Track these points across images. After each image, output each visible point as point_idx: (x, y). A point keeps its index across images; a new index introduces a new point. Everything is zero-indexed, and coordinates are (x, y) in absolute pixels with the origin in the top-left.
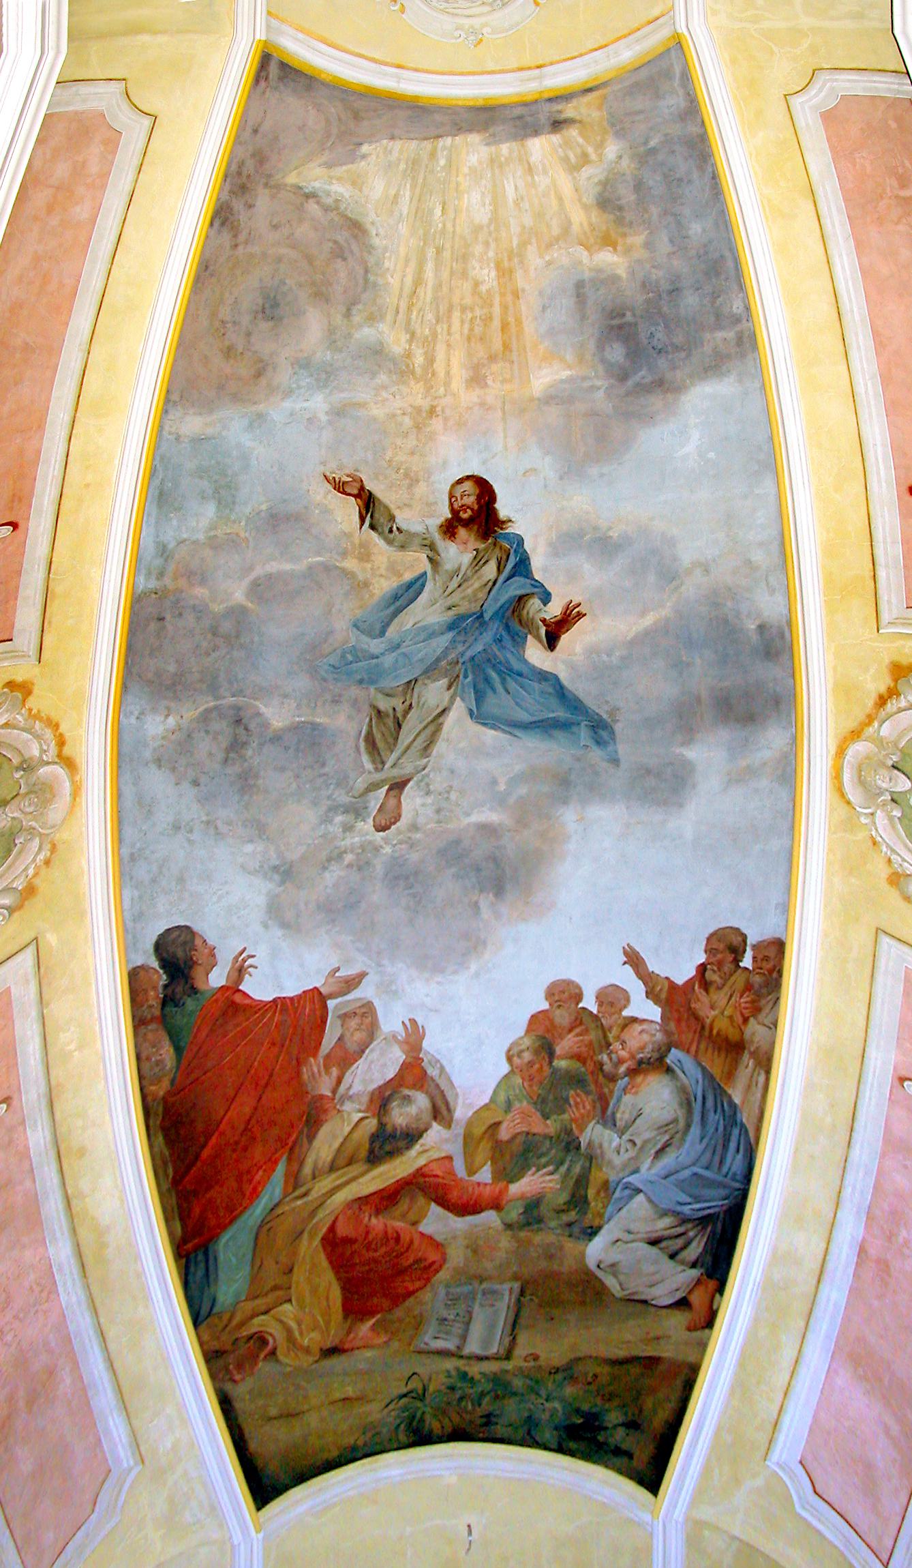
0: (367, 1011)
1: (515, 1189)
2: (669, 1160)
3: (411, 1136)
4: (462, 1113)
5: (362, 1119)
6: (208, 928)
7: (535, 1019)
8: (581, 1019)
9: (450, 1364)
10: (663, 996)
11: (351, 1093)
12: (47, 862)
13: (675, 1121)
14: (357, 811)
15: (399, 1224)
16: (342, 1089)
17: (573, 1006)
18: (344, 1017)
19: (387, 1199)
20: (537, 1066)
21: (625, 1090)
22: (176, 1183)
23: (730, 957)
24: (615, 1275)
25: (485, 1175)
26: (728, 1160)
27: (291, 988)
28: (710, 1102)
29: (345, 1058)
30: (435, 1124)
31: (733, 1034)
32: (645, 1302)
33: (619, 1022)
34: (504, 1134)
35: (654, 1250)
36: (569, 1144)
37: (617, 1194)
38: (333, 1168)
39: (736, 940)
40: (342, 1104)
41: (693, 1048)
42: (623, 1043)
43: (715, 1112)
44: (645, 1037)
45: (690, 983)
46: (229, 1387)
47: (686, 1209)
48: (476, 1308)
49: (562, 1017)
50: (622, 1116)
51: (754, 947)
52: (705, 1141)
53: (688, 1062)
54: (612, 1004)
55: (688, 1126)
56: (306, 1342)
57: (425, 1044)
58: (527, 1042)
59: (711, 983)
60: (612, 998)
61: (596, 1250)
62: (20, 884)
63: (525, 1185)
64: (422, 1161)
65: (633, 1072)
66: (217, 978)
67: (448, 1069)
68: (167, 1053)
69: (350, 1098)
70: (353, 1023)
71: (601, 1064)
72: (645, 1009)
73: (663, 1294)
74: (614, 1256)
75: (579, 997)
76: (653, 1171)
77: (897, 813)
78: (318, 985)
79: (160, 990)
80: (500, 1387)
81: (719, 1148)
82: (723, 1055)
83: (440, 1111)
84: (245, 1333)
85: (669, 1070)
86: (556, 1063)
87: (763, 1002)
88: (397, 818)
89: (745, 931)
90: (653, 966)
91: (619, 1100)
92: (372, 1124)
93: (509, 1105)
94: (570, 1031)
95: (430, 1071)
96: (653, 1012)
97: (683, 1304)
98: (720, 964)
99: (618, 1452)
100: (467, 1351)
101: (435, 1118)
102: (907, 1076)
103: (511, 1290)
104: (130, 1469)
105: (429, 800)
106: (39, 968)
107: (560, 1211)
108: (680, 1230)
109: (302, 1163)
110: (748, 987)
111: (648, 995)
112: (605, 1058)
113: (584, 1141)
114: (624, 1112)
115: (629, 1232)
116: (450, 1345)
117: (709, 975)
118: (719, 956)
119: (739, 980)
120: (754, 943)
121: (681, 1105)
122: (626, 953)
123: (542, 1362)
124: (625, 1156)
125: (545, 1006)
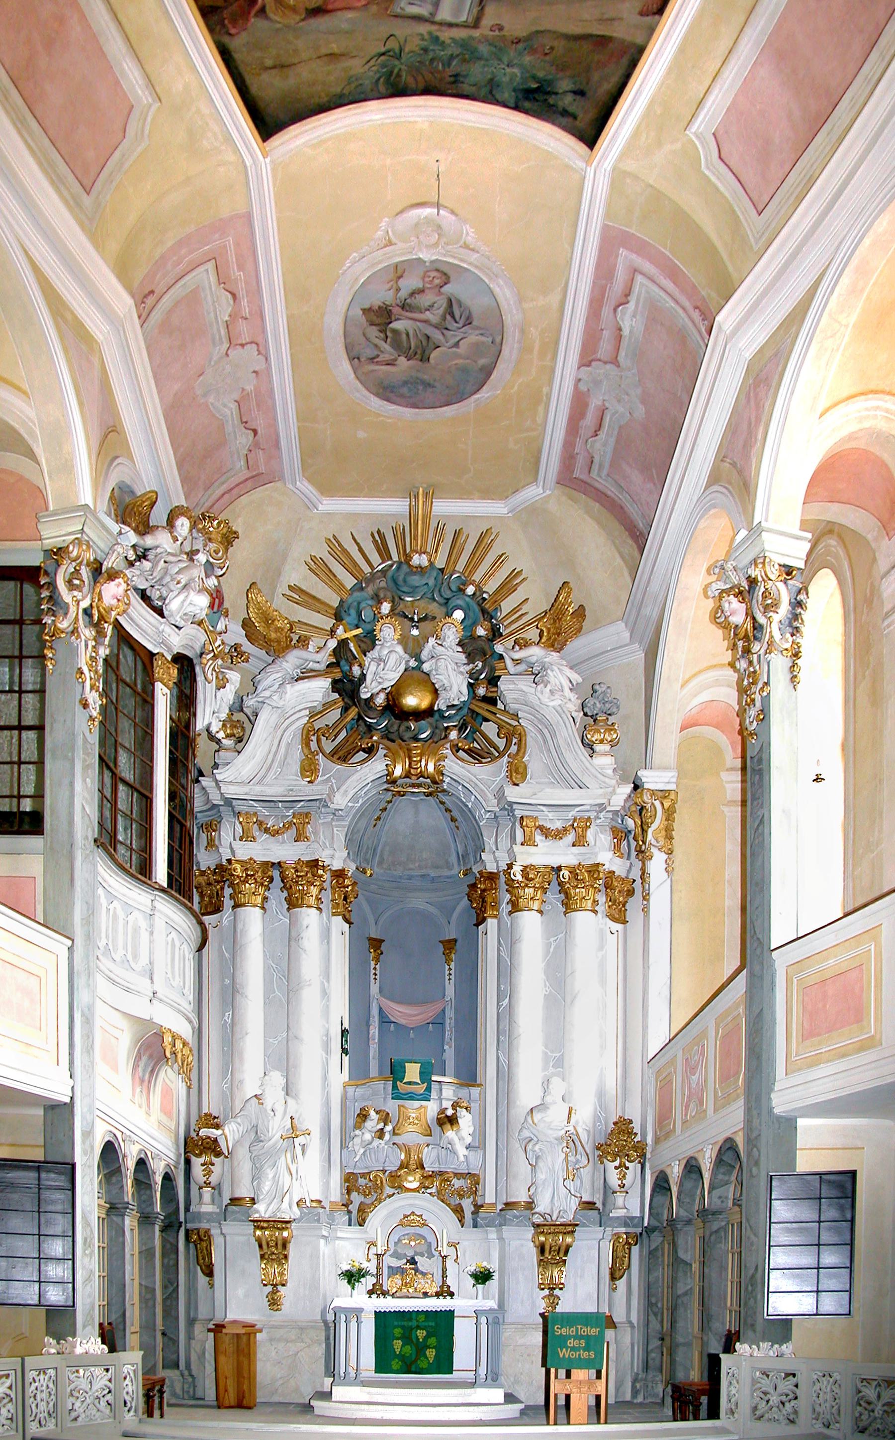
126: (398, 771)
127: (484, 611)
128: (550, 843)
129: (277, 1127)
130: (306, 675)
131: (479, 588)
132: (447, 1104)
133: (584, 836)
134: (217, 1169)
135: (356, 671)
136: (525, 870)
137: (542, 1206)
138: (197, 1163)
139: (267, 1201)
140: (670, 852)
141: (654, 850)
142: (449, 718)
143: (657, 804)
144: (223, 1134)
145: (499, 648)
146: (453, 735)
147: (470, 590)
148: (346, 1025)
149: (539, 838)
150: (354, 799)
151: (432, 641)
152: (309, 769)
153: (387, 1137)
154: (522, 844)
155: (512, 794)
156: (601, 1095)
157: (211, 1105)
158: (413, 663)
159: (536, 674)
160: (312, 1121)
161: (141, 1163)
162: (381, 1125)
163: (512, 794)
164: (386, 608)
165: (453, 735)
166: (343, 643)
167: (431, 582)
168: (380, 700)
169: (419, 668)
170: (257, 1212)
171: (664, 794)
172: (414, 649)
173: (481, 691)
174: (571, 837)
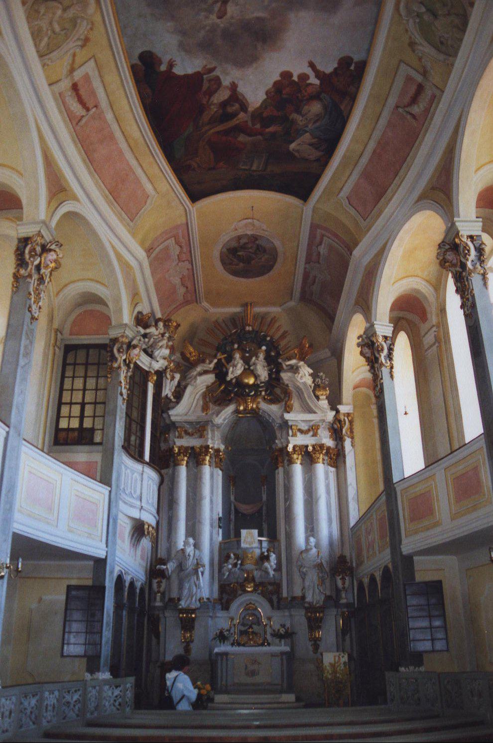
0: (217, 80)
1: (267, 130)
2: (318, 124)
3: (234, 115)
4: (250, 109)
6: (158, 51)
7: (276, 83)
14: (210, 11)
16: (210, 102)
18: (210, 81)
19: (226, 132)
24: (298, 153)
25: (258, 126)
27: (190, 71)
29: (211, 93)
34: (265, 115)
42: (306, 91)
45: (331, 74)
50: (303, 112)
51: (356, 63)
57: (238, 89)
60: (303, 77)
61: (293, 146)
63: (271, 129)
64: (238, 122)
66: (163, 68)
70: (213, 82)
71: (298, 97)
72: (313, 80)
73: (312, 158)
74: (298, 148)
77: (417, 20)
83: (244, 107)
85: (321, 100)
88: (225, 13)
90: (319, 67)
92: (221, 111)
93: (266, 108)
96: (317, 82)
97: (317, 160)
101: (242, 111)
104: (154, 196)
105: (238, 7)
113: (291, 117)
116: (246, 168)
122: (309, 63)
124: (304, 122)
125: (279, 78)
126: (242, 408)
127: (274, 346)
128: (303, 435)
129: (190, 563)
130: (206, 372)
131: (272, 338)
132: (264, 550)
133: (317, 432)
134: (163, 585)
135: (224, 370)
136: (294, 447)
137: (309, 599)
138: (155, 581)
139: (185, 599)
140: (352, 438)
141: (346, 437)
142: (262, 387)
143: (346, 418)
144: (167, 568)
145: (280, 360)
146: (263, 393)
147: (268, 339)
148: (221, 515)
149: (298, 434)
150: (224, 420)
151: (254, 358)
152: (205, 408)
153: (239, 566)
154: (292, 436)
155: (287, 416)
156: (331, 544)
157: (162, 553)
158: (247, 367)
159: (295, 369)
160: (206, 560)
161: (132, 584)
162: (235, 561)
163: (287, 416)
164: (236, 346)
165: (263, 393)
166: (220, 360)
167: (253, 336)
168: (234, 381)
169: (249, 369)
170: (181, 605)
171: (348, 415)
172: (246, 361)
173: (274, 376)
174: (311, 433)
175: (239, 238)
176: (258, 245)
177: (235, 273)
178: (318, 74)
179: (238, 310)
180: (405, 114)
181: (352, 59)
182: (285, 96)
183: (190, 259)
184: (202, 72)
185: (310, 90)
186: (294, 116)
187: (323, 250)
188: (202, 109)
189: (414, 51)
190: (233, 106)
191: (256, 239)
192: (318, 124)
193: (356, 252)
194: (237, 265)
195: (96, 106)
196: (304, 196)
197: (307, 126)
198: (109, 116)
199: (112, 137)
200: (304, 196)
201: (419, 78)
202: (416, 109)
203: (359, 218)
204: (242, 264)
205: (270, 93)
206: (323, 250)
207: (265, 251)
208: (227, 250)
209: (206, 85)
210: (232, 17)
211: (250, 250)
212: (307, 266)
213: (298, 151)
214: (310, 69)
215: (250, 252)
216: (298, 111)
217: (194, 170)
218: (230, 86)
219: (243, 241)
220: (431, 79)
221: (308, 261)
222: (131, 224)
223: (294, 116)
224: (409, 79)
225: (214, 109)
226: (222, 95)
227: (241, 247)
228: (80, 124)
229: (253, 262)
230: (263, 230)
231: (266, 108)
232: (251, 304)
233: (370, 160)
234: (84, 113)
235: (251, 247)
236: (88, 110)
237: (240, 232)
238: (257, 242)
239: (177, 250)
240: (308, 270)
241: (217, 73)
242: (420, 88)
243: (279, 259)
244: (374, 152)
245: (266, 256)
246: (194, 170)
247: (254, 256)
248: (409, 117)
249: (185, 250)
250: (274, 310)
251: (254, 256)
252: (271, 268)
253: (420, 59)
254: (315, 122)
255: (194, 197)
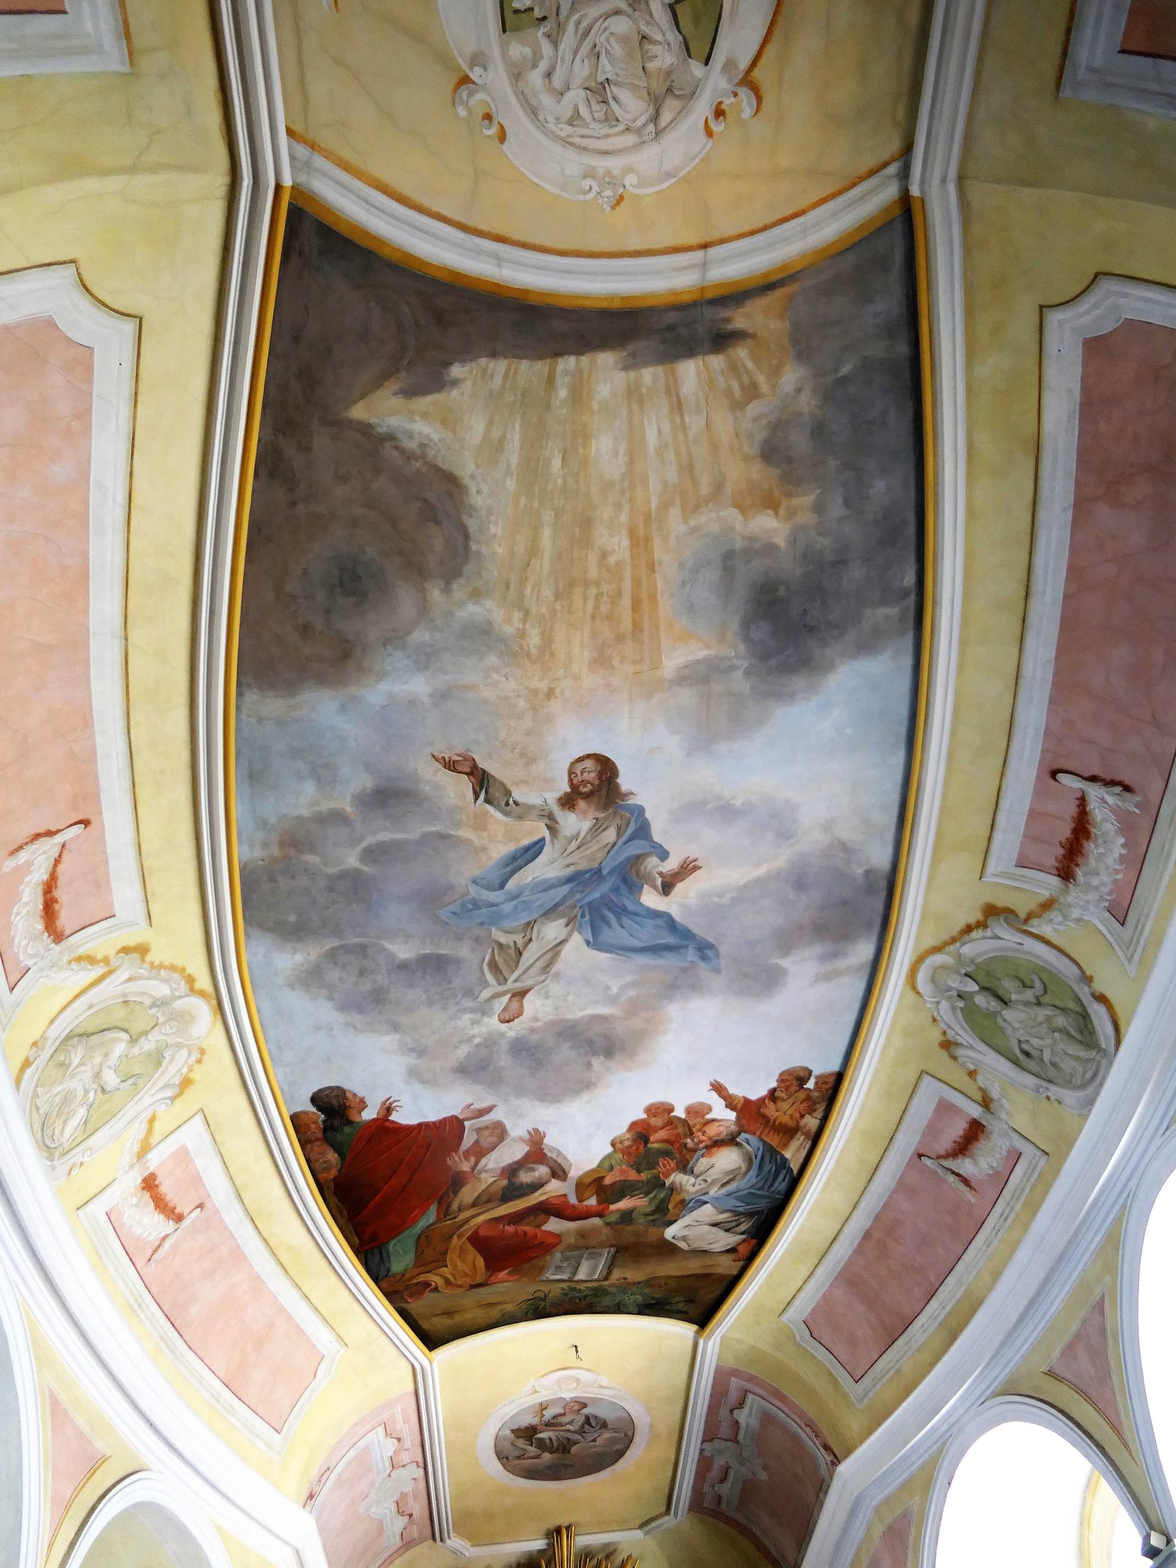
0: (499, 1132)
1: (613, 1207)
2: (732, 1187)
3: (536, 1187)
4: (574, 1173)
5: (496, 1181)
6: (354, 1084)
7: (633, 1125)
8: (672, 1122)
9: (564, 1285)
10: (739, 1106)
11: (486, 1168)
12: (199, 1062)
13: (740, 1168)
14: (484, 1010)
15: (526, 1228)
16: (480, 1166)
17: (666, 1115)
18: (479, 1130)
20: (634, 1148)
21: (703, 1156)
22: (351, 1219)
23: (795, 1083)
24: (684, 1241)
25: (592, 1201)
26: (776, 1184)
27: (433, 1116)
28: (767, 1160)
29: (479, 1151)
30: (553, 1180)
31: (792, 1124)
32: (705, 1251)
33: (702, 1121)
34: (608, 1181)
35: (714, 1229)
36: (656, 1184)
37: (691, 1204)
38: (474, 1205)
39: (802, 1074)
40: (480, 1173)
41: (758, 1133)
42: (704, 1133)
43: (770, 1163)
44: (722, 1129)
45: (762, 1101)
46: (404, 1305)
47: (741, 1209)
48: (583, 1261)
49: (657, 1122)
50: (697, 1170)
51: (817, 1077)
52: (759, 1178)
53: (754, 1140)
54: (697, 1113)
55: (748, 1170)
56: (459, 1283)
58: (628, 1136)
59: (778, 1098)
60: (698, 1111)
61: (670, 1232)
62: (176, 1081)
63: (624, 1204)
65: (708, 1148)
67: (564, 1152)
68: (332, 1157)
69: (485, 1171)
70: (486, 1133)
71: (685, 1144)
72: (723, 1114)
73: (717, 1247)
74: (685, 1233)
75: (672, 1110)
76: (718, 1193)
77: (961, 1004)
78: (455, 1114)
79: (321, 1123)
80: (599, 1292)
81: (771, 1180)
82: (781, 1135)
83: (559, 1172)
84: (415, 1281)
85: (738, 1144)
86: (649, 1146)
87: (818, 1106)
88: (520, 1014)
89: (811, 1068)
90: (732, 1090)
91: (697, 1160)
92: (505, 1182)
93: (612, 1168)
94: (662, 1128)
95: (549, 1155)
96: (732, 1115)
97: (733, 1250)
98: (787, 1088)
99: (678, 1312)
100: (576, 1278)
101: (554, 1177)
102: (925, 1153)
103: (608, 1252)
105: (549, 1002)
106: (209, 1126)
107: (646, 1215)
108: (737, 1218)
109: (449, 1206)
110: (808, 1099)
111: (726, 1107)
112: (689, 1141)
113: (668, 1182)
114: (700, 1167)
115: (697, 1221)
116: (565, 1277)
117: (777, 1094)
118: (788, 1083)
119: (801, 1095)
120: (818, 1074)
121: (744, 1161)
122: (712, 1085)
123: (628, 1280)
124: (697, 1188)
125: (644, 1116)
175: (543, 1407)
176: (587, 1418)
177: (532, 1474)
178: (730, 1102)
179: (539, 1544)
180: (939, 1170)
181: (810, 1073)
182: (656, 1146)
183: (420, 1460)
184: (461, 1117)
185: (712, 1131)
186: (678, 1178)
187: (742, 1416)
188: (458, 1181)
189: (954, 1058)
190: (533, 1170)
191: (584, 1405)
192: (732, 1187)
193: (843, 1469)
194: (538, 1457)
195: (201, 1206)
196: (703, 1318)
197: (707, 1193)
198: (233, 1217)
199: (238, 1256)
200: (703, 1318)
201: (975, 1111)
202: (965, 1166)
203: (846, 1381)
204: (547, 1456)
205: (621, 1142)
206: (742, 1416)
207: (604, 1425)
208: (513, 1431)
209: (468, 1140)
210: (536, 1019)
211: (568, 1427)
212: (707, 1446)
213: (684, 1239)
214: (714, 1094)
215: (569, 1431)
216: (684, 1167)
217: (436, 1289)
218: (527, 1136)
219: (548, 1414)
220: (1004, 1116)
221: (709, 1436)
222: (277, 1439)
223: (678, 1178)
224: (944, 1108)
225: (487, 1179)
226: (511, 1152)
227: (548, 1424)
228: (156, 1256)
229: (574, 1449)
230: (601, 1387)
231: (612, 1168)
232: (568, 1528)
233: (860, 1250)
234: (171, 1225)
235: (571, 1422)
236: (179, 1218)
237: (544, 1396)
238: (585, 1411)
239: (390, 1446)
240: (707, 1454)
241: (495, 1116)
242: (975, 1130)
243: (637, 1439)
244: (867, 1235)
245: (607, 1435)
246: (436, 1289)
247: (577, 1437)
248: (951, 1178)
249: (408, 1443)
250: (628, 1540)
251: (577, 1437)
252: (621, 1454)
253: (972, 1074)
254: (723, 1185)
255: (431, 1341)
